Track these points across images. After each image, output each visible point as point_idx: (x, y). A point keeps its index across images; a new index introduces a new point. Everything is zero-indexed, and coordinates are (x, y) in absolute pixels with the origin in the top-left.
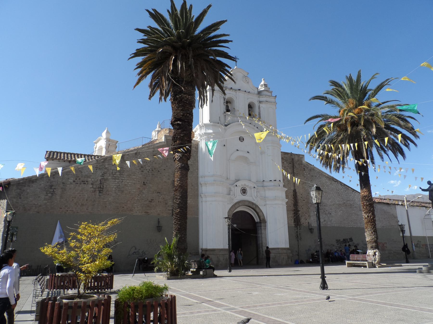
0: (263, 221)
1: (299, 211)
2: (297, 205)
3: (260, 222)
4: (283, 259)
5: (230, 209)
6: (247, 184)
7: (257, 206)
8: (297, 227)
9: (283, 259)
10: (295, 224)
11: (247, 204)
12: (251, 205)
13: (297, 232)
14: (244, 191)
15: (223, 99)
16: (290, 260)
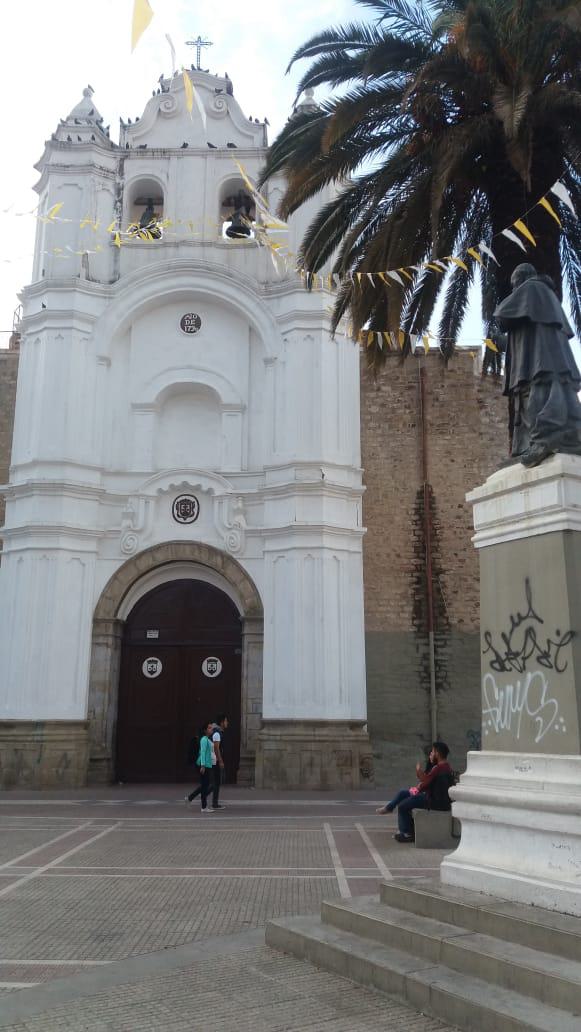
0: (257, 615)
1: (442, 571)
2: (436, 549)
3: (244, 619)
4: (311, 764)
5: (115, 577)
6: (193, 481)
7: (230, 559)
8: (428, 637)
9: (311, 764)
10: (419, 626)
11: (187, 553)
12: (204, 558)
13: (426, 657)
14: (185, 510)
15: (112, 191)
16: (356, 772)
